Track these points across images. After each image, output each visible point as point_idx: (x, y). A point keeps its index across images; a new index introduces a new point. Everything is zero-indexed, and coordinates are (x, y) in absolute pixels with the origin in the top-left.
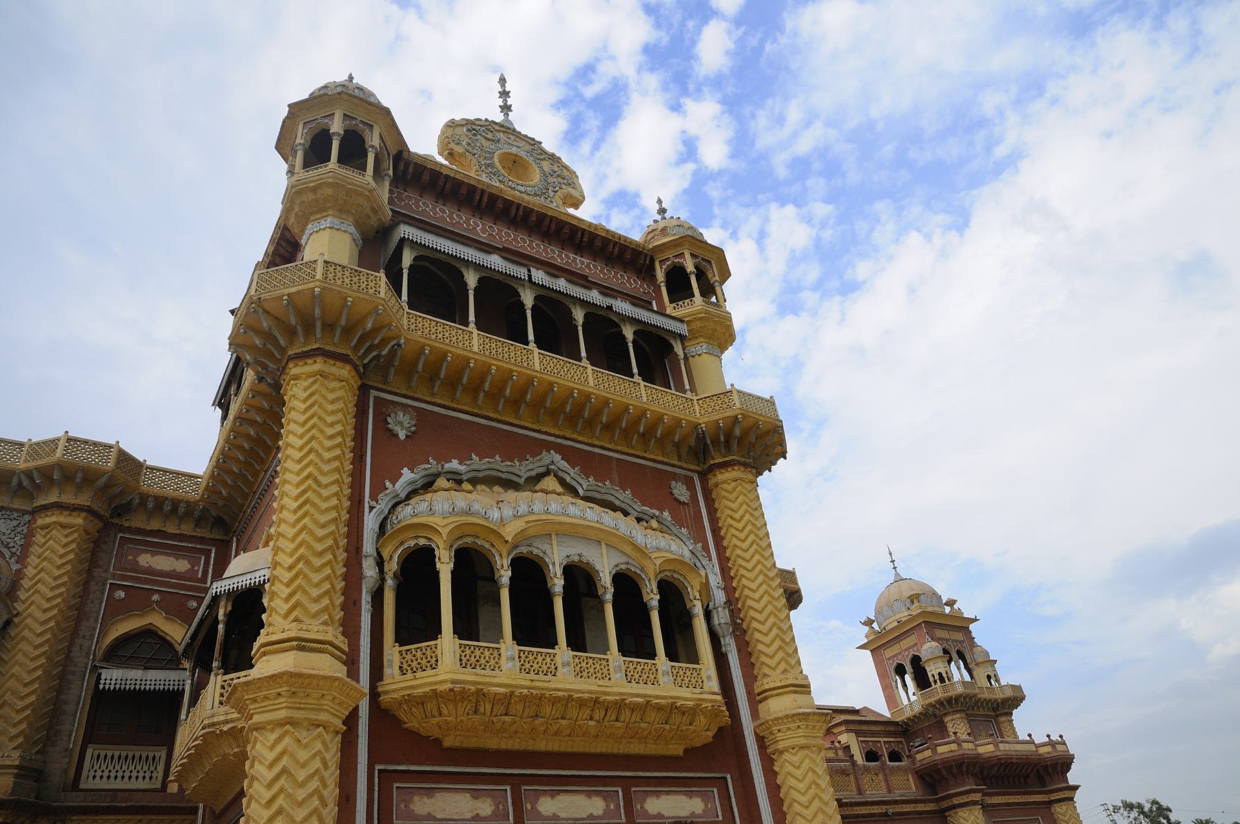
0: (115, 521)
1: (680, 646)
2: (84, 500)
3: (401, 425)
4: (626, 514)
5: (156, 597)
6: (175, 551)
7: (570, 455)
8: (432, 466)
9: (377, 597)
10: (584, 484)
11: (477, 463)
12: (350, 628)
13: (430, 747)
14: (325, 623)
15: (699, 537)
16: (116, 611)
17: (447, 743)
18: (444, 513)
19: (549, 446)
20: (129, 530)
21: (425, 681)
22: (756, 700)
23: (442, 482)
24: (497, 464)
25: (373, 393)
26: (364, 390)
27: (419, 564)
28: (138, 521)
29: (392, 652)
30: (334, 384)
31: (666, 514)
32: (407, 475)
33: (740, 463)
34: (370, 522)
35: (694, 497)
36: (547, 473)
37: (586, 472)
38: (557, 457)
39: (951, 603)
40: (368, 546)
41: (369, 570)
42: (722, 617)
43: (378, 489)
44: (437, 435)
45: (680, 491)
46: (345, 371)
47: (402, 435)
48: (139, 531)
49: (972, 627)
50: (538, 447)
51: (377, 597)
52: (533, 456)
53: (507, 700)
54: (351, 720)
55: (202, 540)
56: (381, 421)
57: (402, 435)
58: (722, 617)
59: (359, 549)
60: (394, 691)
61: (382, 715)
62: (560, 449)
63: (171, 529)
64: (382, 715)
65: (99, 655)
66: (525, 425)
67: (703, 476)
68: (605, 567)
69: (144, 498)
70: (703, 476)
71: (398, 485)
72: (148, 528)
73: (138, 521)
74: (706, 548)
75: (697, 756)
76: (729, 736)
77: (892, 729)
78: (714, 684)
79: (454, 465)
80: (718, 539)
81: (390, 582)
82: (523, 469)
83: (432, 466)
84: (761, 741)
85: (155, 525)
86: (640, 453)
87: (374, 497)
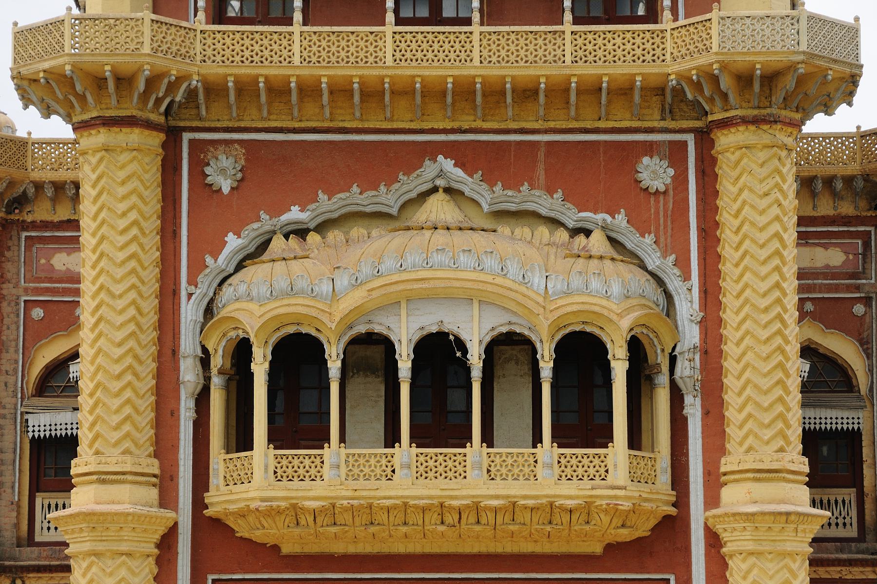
0: (12, 217)
1: (582, 426)
3: (223, 174)
7: (466, 156)
9: (202, 399)
10: (489, 196)
11: (327, 204)
12: (163, 447)
14: (126, 452)
17: (286, 550)
18: (261, 302)
19: (431, 151)
20: (34, 226)
23: (278, 243)
24: (357, 197)
25: (186, 137)
26: (172, 135)
29: (218, 457)
30: (124, 157)
31: (621, 220)
32: (233, 242)
33: (745, 121)
34: (190, 312)
35: (680, 180)
36: (435, 190)
37: (489, 180)
38: (447, 164)
40: (188, 344)
41: (189, 373)
43: (197, 267)
44: (275, 169)
45: (654, 173)
46: (134, 136)
47: (226, 190)
48: (46, 225)
50: (417, 155)
51: (202, 399)
52: (407, 173)
53: (330, 512)
54: (167, 542)
57: (226, 190)
59: (175, 352)
60: (218, 503)
61: (210, 530)
62: (451, 150)
65: (30, 388)
66: (401, 124)
68: (474, 333)
69: (39, 186)
71: (221, 258)
72: (56, 219)
74: (683, 264)
76: (672, 528)
79: (295, 214)
81: (217, 382)
82: (388, 198)
83: (266, 222)
84: (713, 540)
86: (588, 125)
87: (192, 281)
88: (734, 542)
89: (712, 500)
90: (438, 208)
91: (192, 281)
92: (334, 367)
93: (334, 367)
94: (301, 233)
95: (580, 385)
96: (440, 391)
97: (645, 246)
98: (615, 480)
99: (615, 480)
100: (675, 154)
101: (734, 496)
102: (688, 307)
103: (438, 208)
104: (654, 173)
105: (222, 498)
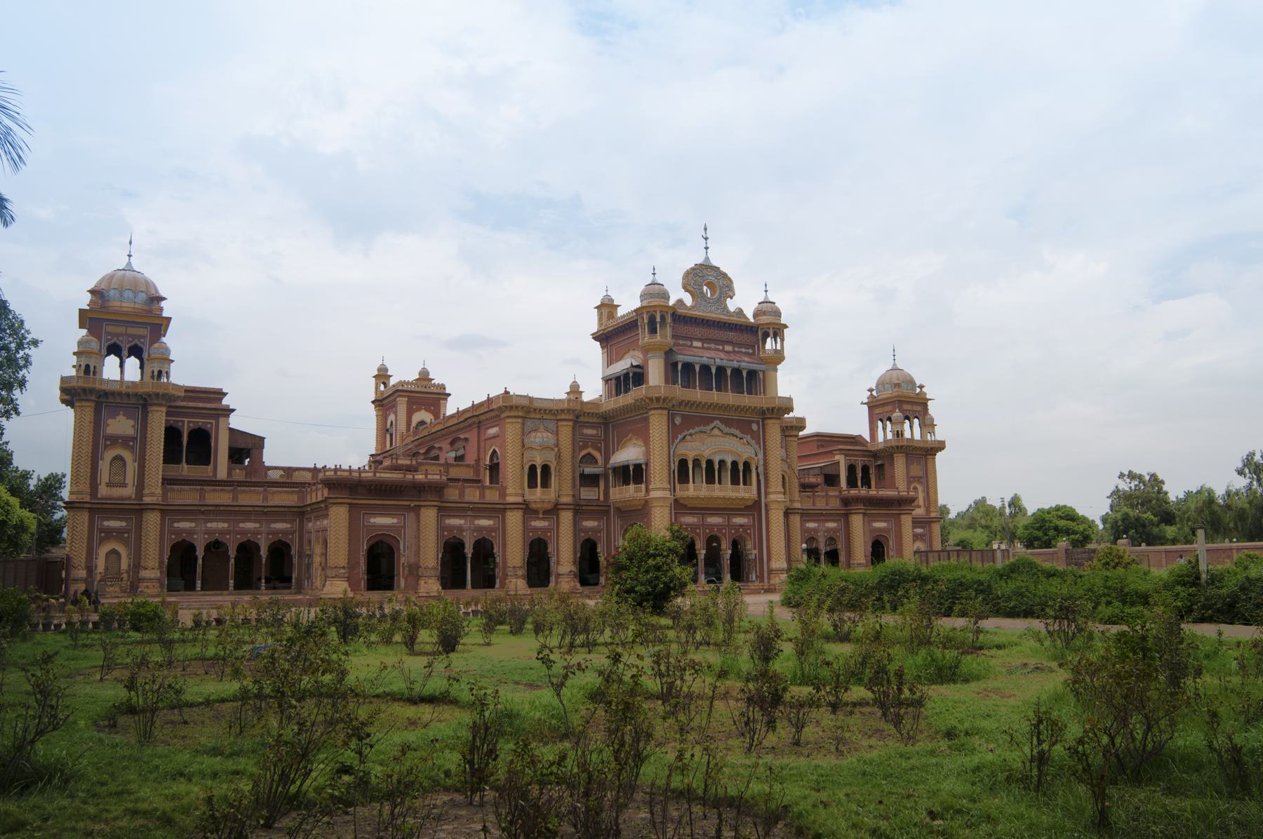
2: (571, 417)
3: (678, 421)
6: (592, 428)
7: (723, 421)
10: (726, 430)
11: (697, 429)
13: (685, 507)
15: (758, 443)
16: (581, 450)
19: (715, 419)
21: (685, 494)
22: (767, 494)
28: (581, 419)
29: (678, 486)
39: (921, 387)
42: (761, 469)
49: (929, 403)
50: (711, 420)
58: (761, 469)
64: (676, 501)
67: (763, 420)
70: (763, 420)
73: (581, 419)
75: (748, 508)
78: (755, 492)
80: (765, 445)
88: (772, 506)
90: (716, 432)
92: (690, 467)
93: (690, 467)
95: (740, 473)
96: (711, 472)
97: (753, 442)
98: (745, 493)
99: (745, 493)
100: (758, 423)
101: (772, 497)
102: (761, 456)
103: (716, 432)
104: (755, 427)
105: (679, 494)
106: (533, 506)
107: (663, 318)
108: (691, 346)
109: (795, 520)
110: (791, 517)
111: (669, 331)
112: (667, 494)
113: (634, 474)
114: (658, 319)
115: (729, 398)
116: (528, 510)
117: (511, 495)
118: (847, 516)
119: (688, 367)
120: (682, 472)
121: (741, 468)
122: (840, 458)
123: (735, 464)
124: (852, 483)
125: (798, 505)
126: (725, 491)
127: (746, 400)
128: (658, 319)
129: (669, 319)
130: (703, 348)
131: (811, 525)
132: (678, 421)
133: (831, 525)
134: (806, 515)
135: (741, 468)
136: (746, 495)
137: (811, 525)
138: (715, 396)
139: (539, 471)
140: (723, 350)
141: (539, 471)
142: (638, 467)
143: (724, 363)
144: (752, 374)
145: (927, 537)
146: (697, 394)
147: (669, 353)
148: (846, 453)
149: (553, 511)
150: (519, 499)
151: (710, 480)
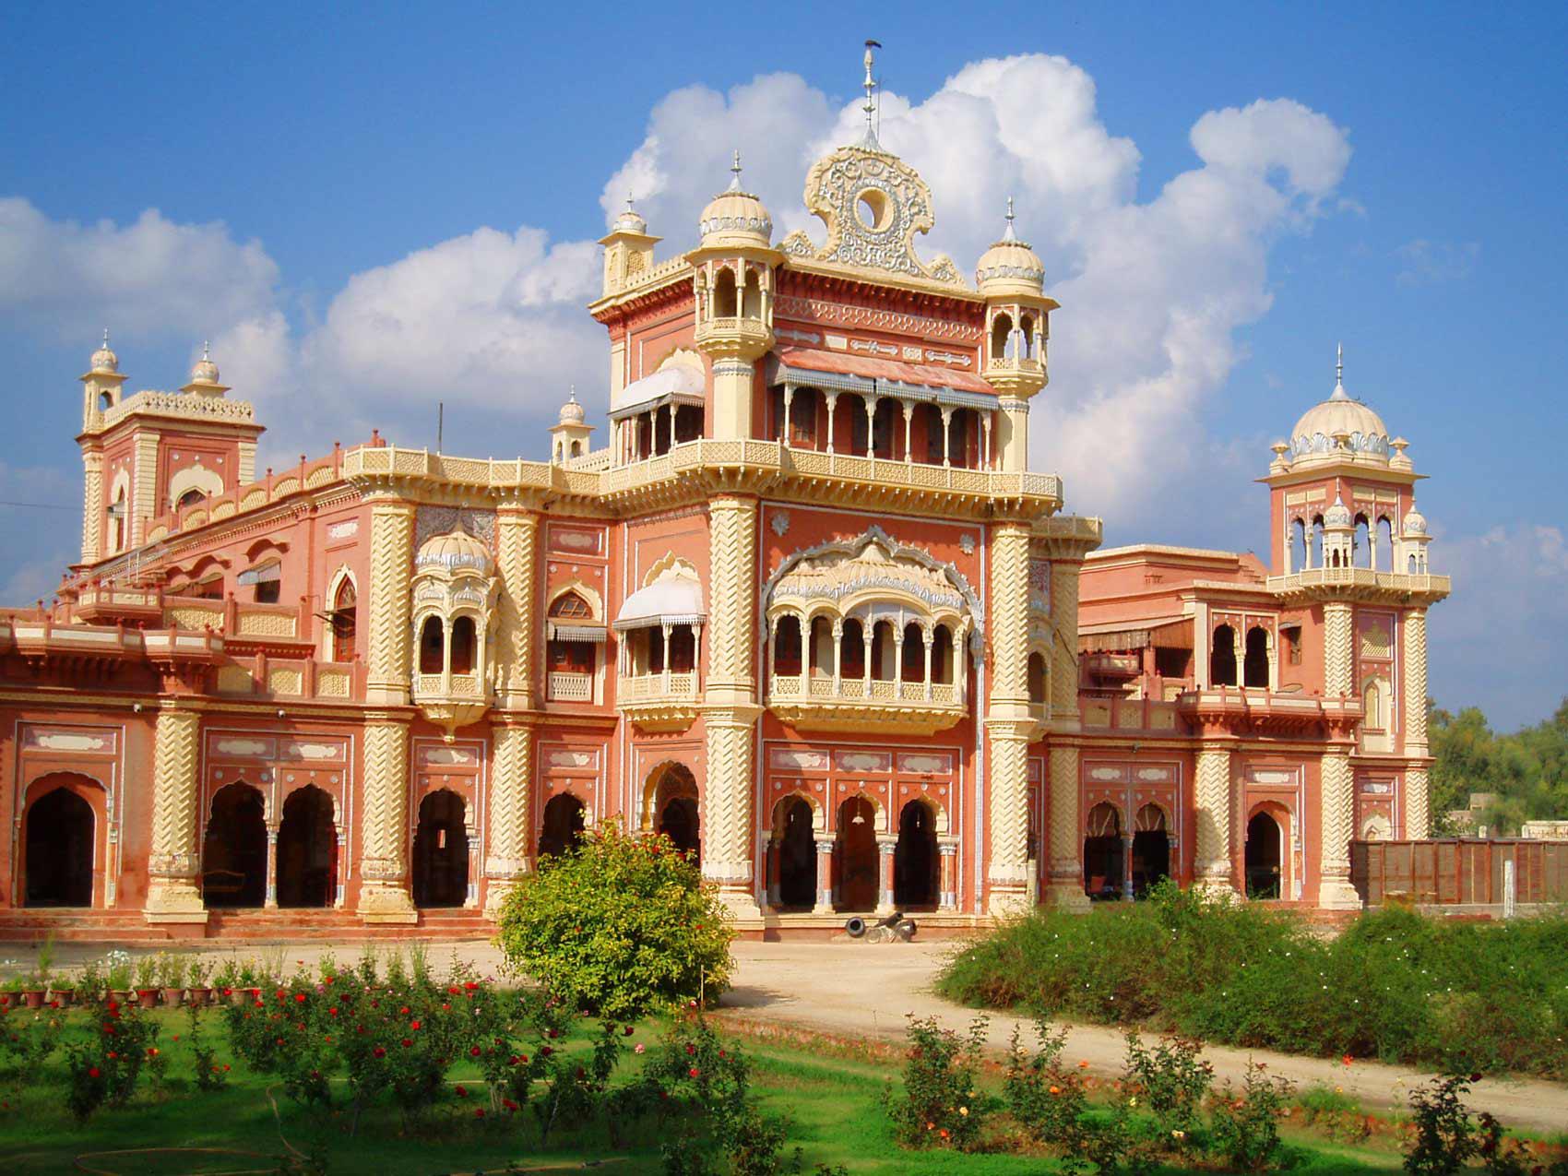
3: (780, 526)
4: (922, 566)
5: (575, 569)
8: (797, 556)
19: (873, 521)
20: (553, 517)
27: (789, 625)
29: (774, 679)
48: (560, 518)
55: (599, 521)
56: (769, 524)
63: (578, 514)
73: (556, 510)
74: (977, 591)
75: (941, 735)
77: (1263, 600)
85: (566, 513)
89: (986, 713)
91: (765, 583)
94: (810, 560)
95: (926, 652)
96: (857, 647)
99: (937, 700)
106: (432, 715)
107: (751, 278)
108: (821, 346)
109: (1066, 763)
110: (1057, 754)
111: (766, 315)
112: (745, 700)
113: (670, 647)
114: (740, 281)
115: (907, 474)
116: (417, 725)
117: (377, 686)
118: (1191, 756)
119: (809, 399)
120: (781, 647)
121: (928, 638)
122: (1195, 610)
123: (913, 631)
124: (1222, 671)
125: (1074, 727)
126: (890, 695)
127: (945, 479)
128: (740, 281)
129: (765, 281)
130: (848, 352)
131: (1105, 774)
132: (780, 526)
133: (1153, 774)
134: (1091, 751)
135: (928, 638)
136: (938, 707)
137: (1105, 774)
138: (870, 469)
139: (447, 632)
140: (898, 359)
141: (447, 632)
142: (683, 636)
143: (899, 390)
144: (966, 419)
145: (1394, 806)
146: (825, 463)
147: (763, 363)
148: (1213, 599)
149: (481, 730)
150: (399, 699)
151: (852, 668)
